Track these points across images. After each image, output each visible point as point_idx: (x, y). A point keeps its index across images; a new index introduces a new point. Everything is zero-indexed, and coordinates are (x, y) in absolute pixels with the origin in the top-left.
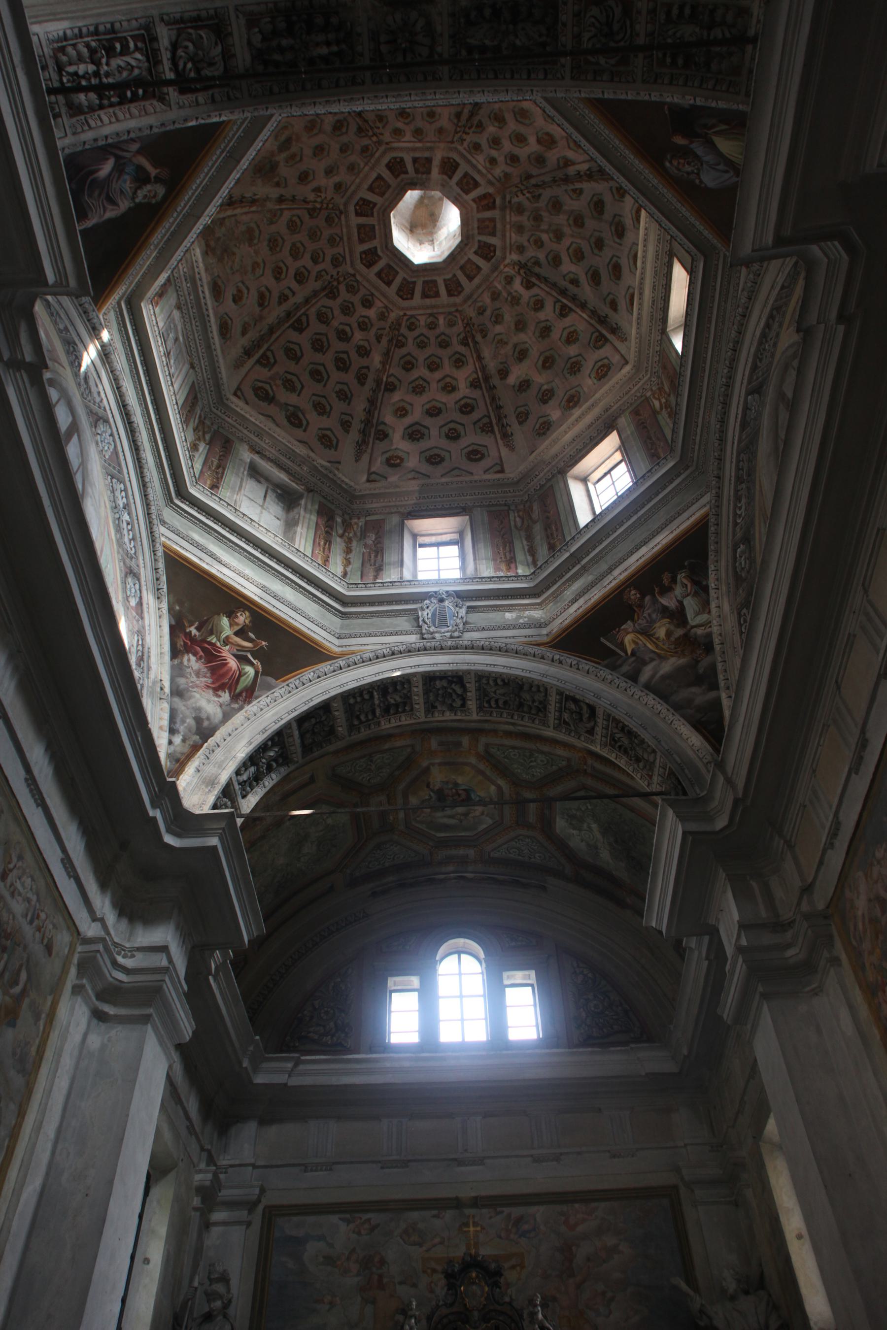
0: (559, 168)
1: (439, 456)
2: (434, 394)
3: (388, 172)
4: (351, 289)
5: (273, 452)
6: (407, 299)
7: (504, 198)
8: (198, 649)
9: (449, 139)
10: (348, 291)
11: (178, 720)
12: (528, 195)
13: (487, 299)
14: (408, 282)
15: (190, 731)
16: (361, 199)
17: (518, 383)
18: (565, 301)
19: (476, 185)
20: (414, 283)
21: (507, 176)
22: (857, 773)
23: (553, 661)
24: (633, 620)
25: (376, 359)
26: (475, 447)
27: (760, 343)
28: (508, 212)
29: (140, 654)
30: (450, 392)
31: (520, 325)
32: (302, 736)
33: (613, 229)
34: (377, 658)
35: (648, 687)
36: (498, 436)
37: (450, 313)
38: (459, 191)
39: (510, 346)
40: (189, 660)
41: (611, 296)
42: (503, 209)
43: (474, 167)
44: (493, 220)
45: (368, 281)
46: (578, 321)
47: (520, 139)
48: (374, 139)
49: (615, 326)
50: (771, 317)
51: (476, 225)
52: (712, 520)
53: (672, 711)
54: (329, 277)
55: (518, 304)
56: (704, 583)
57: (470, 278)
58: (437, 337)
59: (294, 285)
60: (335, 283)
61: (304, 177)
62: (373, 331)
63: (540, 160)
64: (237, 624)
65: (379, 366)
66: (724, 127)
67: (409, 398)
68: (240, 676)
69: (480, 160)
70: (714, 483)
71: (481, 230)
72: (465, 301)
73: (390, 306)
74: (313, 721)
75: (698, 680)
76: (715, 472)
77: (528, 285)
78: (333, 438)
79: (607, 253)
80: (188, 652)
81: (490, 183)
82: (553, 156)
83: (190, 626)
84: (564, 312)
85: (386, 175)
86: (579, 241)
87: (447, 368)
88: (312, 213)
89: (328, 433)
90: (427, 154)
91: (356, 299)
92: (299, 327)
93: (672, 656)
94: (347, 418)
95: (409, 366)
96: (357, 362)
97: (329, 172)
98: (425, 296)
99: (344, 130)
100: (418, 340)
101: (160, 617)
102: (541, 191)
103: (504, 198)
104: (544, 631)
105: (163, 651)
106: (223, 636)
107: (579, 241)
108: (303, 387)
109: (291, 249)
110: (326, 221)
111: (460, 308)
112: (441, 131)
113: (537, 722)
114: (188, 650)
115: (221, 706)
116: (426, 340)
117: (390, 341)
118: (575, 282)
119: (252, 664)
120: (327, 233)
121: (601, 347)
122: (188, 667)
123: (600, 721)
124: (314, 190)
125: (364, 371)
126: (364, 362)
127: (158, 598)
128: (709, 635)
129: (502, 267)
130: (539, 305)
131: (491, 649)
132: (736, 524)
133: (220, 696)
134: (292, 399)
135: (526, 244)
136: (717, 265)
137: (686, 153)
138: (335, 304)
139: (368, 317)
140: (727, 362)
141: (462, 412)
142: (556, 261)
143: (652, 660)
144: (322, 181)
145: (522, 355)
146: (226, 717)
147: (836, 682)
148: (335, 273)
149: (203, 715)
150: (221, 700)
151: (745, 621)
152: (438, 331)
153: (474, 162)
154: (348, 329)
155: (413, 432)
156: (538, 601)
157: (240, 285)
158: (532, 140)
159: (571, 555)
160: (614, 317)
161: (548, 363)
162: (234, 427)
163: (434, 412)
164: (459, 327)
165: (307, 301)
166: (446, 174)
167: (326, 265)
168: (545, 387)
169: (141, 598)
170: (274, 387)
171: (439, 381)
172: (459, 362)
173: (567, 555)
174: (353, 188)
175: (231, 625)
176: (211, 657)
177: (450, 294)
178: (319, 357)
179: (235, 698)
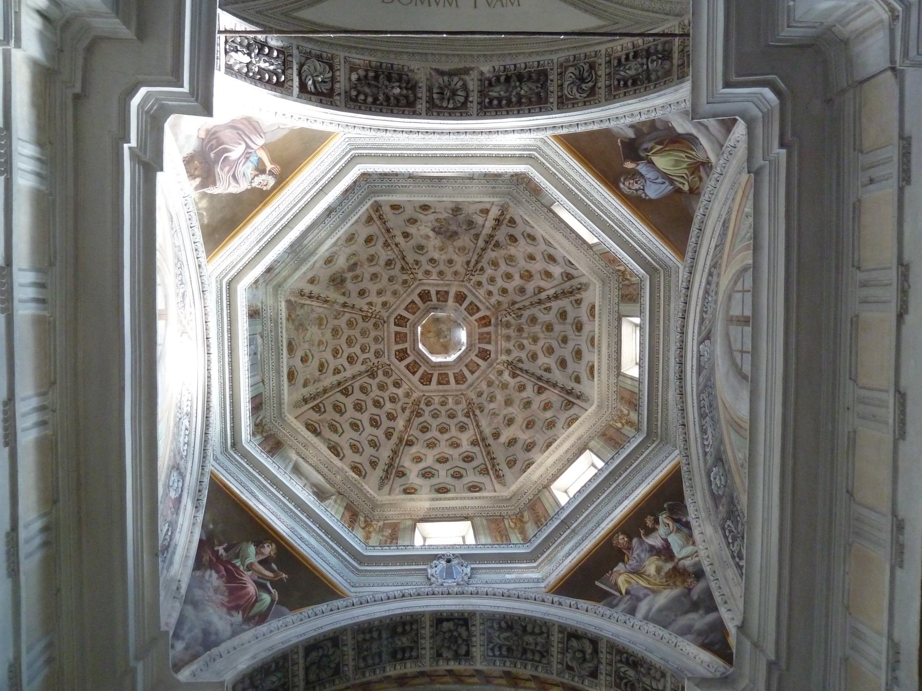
0: (535, 294)
1: (445, 488)
2: (443, 448)
3: (419, 299)
4: (386, 374)
5: (314, 460)
7: (497, 318)
8: (222, 568)
9: (461, 279)
10: (384, 374)
11: (186, 627)
12: (513, 315)
13: (484, 386)
16: (399, 315)
17: (507, 441)
18: (541, 384)
19: (478, 309)
20: (432, 374)
21: (499, 303)
22: (901, 567)
23: (553, 603)
24: (623, 561)
25: (400, 424)
26: (475, 484)
27: (704, 298)
28: (499, 327)
29: (166, 543)
30: (456, 447)
31: (508, 402)
32: (307, 669)
33: (574, 327)
34: (389, 598)
35: (646, 618)
36: (493, 477)
37: (457, 395)
38: (466, 313)
39: (502, 416)
40: (210, 576)
41: (575, 374)
42: (496, 325)
43: (476, 297)
44: (489, 333)
46: (552, 395)
47: (508, 276)
48: (412, 276)
49: (579, 394)
50: (710, 274)
51: (477, 337)
52: (684, 469)
53: (674, 635)
54: (371, 364)
55: (507, 388)
56: (684, 520)
57: (472, 373)
58: (447, 411)
59: (346, 364)
60: (375, 369)
61: (362, 293)
62: (400, 404)
63: (522, 290)
64: (262, 554)
65: (402, 428)
66: (659, 147)
67: (425, 451)
68: (256, 601)
69: (481, 293)
70: (680, 430)
71: (481, 340)
72: (468, 388)
73: (414, 389)
74: (321, 652)
75: (695, 606)
76: (680, 422)
77: (514, 376)
78: (362, 470)
79: (571, 345)
80: (211, 568)
81: (488, 308)
82: (530, 287)
83: (219, 546)
84: (540, 390)
85: (418, 300)
86: (550, 341)
87: (454, 432)
88: (364, 318)
89: (359, 466)
90: (446, 289)
91: (389, 381)
92: (346, 393)
93: (665, 589)
94: (375, 459)
95: (424, 429)
96: (386, 423)
97: (379, 293)
98: (439, 383)
99: (392, 266)
100: (433, 413)
101: (194, 524)
102: (523, 312)
103: (497, 318)
104: (542, 585)
105: (189, 554)
106: (248, 562)
107: (550, 341)
108: (343, 432)
109: (347, 339)
110: (374, 325)
111: (464, 393)
112: (456, 273)
113: (540, 669)
114: (212, 566)
115: (232, 625)
116: (438, 413)
117: (413, 412)
118: (548, 370)
119: (270, 593)
120: (373, 334)
121: (571, 408)
122: (209, 582)
123: (603, 656)
124: (367, 304)
125: (391, 430)
126: (391, 424)
127: (196, 507)
128: (698, 564)
129: (495, 365)
130: (522, 388)
131: (494, 595)
132: (705, 453)
133: (232, 616)
134: (334, 437)
135: (512, 348)
136: (659, 281)
137: (634, 175)
138: (374, 383)
139: (397, 394)
140: (679, 329)
141: (465, 461)
142: (534, 357)
143: (646, 595)
144: (373, 298)
145: (510, 422)
146: (234, 634)
147: (848, 492)
148: (376, 361)
150: (233, 619)
151: (731, 531)
152: (447, 407)
153: (477, 294)
154: (381, 400)
155: (426, 473)
156: (535, 565)
157: (308, 351)
158: (517, 277)
159: (562, 521)
160: (578, 388)
161: (530, 425)
162: (287, 436)
163: (443, 460)
164: (464, 405)
165: (354, 377)
166: (457, 302)
167: (371, 355)
168: (529, 441)
170: (322, 427)
171: (447, 440)
172: (462, 428)
173: (557, 522)
174: (394, 307)
175: (257, 554)
176: (232, 577)
177: (457, 382)
178: (358, 415)
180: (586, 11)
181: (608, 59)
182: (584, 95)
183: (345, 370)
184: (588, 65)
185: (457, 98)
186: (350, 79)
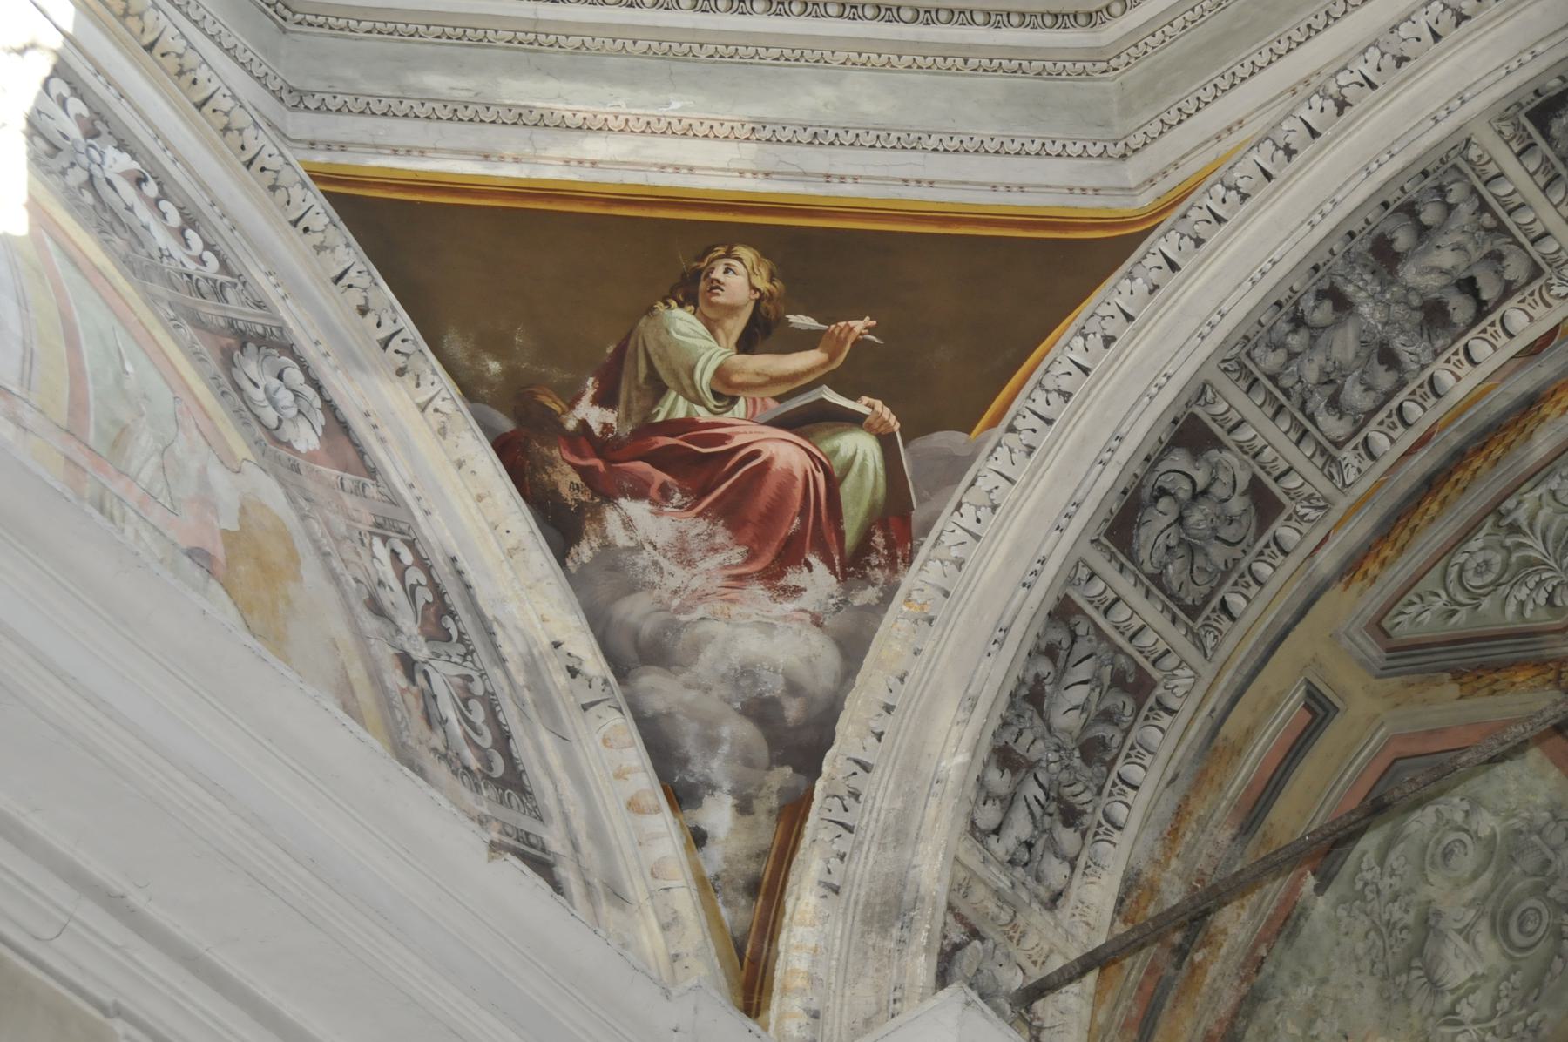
11: (690, 746)
15: (749, 763)
40: (628, 524)
64: (732, 310)
68: (833, 483)
80: (609, 498)
106: (704, 378)
114: (604, 490)
115: (817, 622)
119: (855, 421)
122: (639, 548)
133: (797, 591)
149: (773, 686)
150: (808, 601)
169: (329, 407)
175: (711, 326)
179: (852, 567)
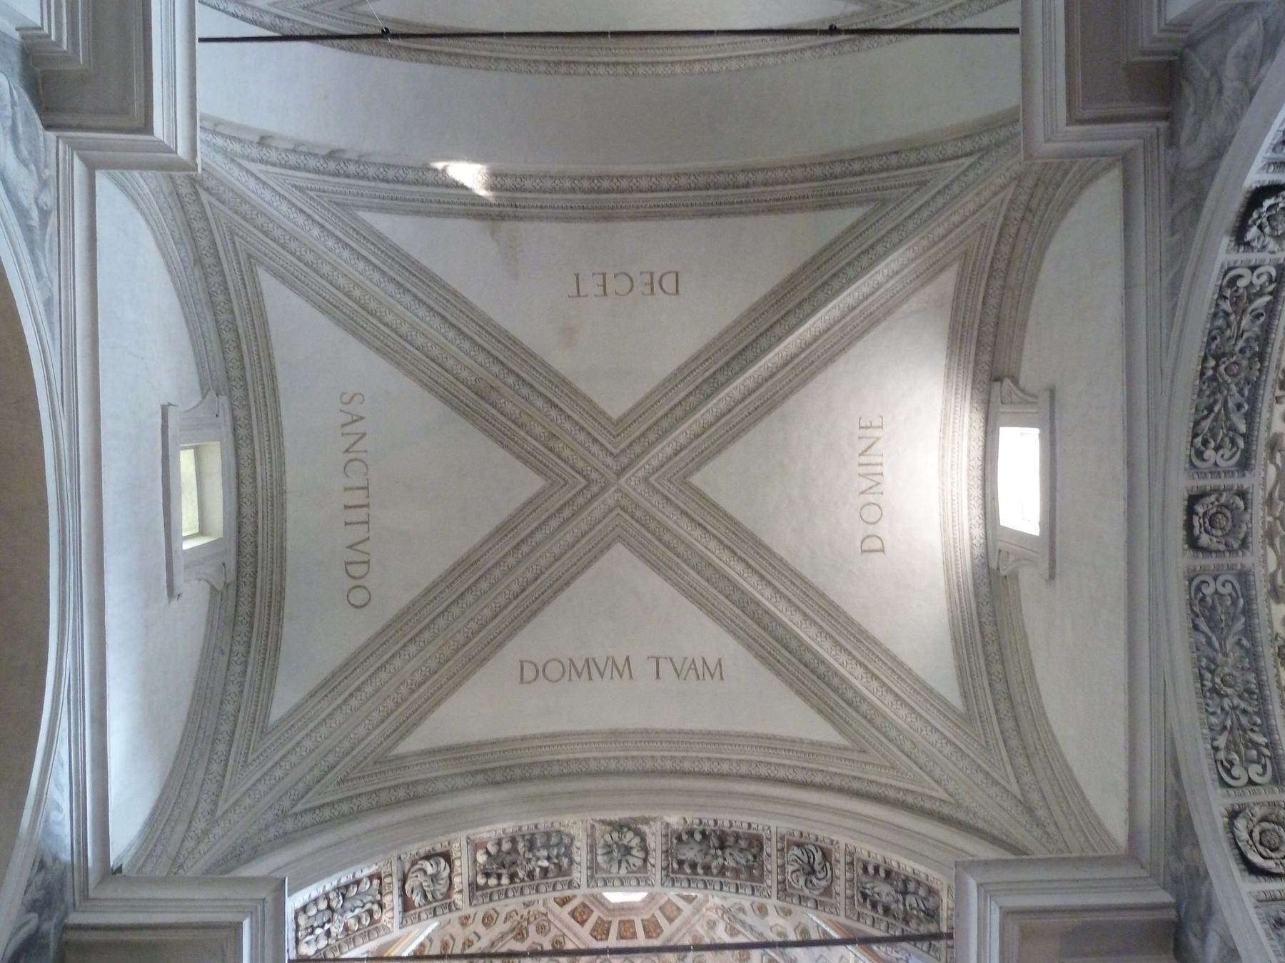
6: (601, 939)
10: (538, 932)
14: (603, 921)
20: (610, 923)
45: (560, 920)
57: (670, 920)
59: (481, 929)
60: (525, 924)
129: (704, 910)
148: (525, 913)
180: (821, 712)
181: (848, 859)
182: (816, 892)
183: (479, 938)
184: (820, 853)
185: (631, 860)
186: (475, 861)
